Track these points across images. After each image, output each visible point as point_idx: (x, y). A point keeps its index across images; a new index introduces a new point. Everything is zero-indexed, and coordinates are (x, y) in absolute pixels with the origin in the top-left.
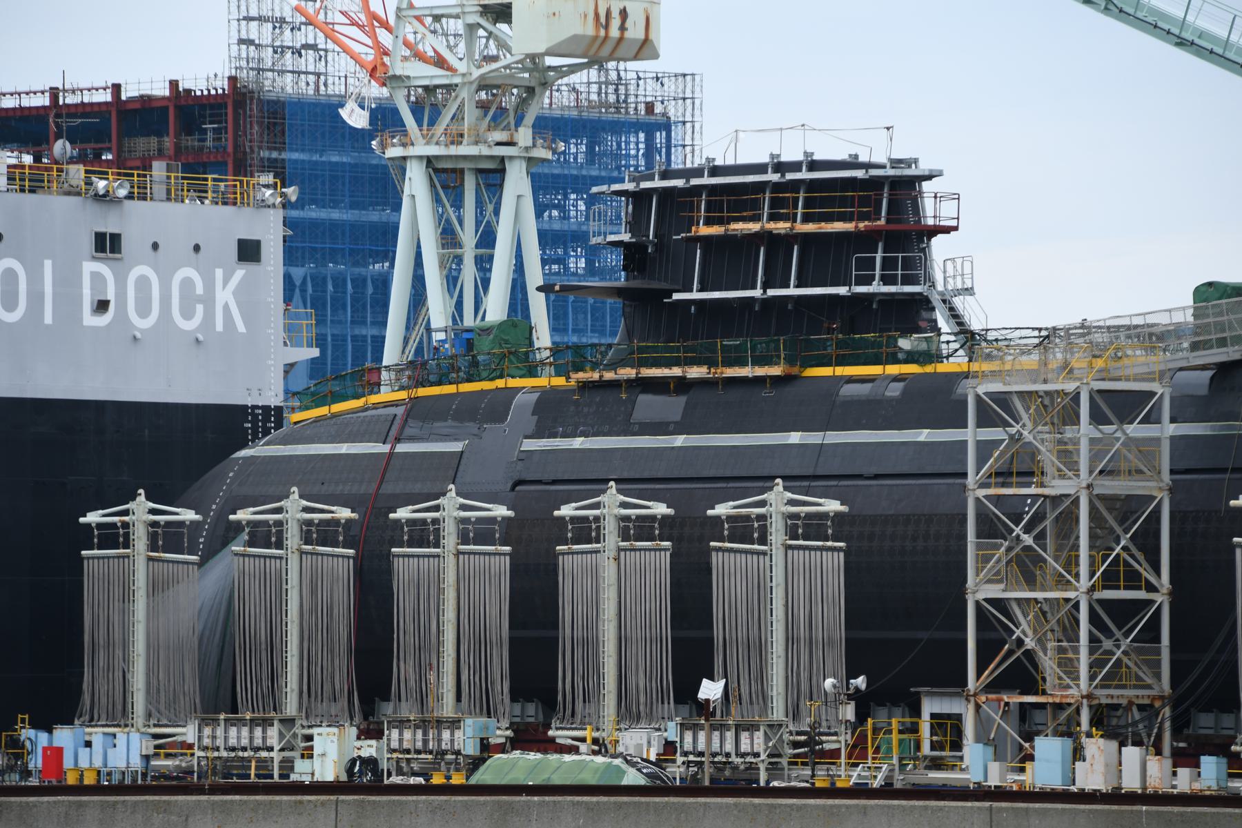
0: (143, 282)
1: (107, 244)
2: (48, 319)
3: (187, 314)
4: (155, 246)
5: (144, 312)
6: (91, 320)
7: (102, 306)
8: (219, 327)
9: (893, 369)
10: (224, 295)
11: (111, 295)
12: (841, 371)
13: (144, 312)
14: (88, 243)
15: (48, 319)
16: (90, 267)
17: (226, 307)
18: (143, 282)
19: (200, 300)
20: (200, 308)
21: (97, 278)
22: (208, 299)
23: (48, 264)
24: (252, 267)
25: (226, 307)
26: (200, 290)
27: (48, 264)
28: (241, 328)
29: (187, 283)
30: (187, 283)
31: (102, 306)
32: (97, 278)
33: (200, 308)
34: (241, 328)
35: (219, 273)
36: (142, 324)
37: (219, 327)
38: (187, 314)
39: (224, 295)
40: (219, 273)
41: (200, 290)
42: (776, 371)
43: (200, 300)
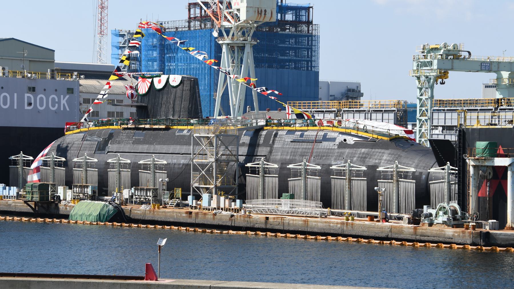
0: (41, 99)
1: (32, 90)
2: (15, 107)
3: (53, 106)
4: (45, 90)
5: (41, 105)
6: (27, 107)
7: (30, 104)
8: (62, 109)
10: (63, 102)
11: (33, 102)
13: (41, 105)
15: (15, 107)
16: (27, 95)
17: (64, 104)
18: (41, 99)
19: (57, 103)
20: (57, 105)
21: (29, 98)
22: (59, 103)
23: (16, 94)
24: (71, 95)
25: (64, 104)
26: (57, 100)
27: (16, 94)
28: (68, 109)
29: (53, 99)
30: (53, 99)
31: (30, 104)
32: (29, 98)
33: (57, 105)
34: (68, 109)
35: (62, 96)
37: (62, 109)
38: (53, 106)
39: (63, 102)
40: (62, 96)
41: (57, 100)
42: (164, 127)
43: (57, 103)
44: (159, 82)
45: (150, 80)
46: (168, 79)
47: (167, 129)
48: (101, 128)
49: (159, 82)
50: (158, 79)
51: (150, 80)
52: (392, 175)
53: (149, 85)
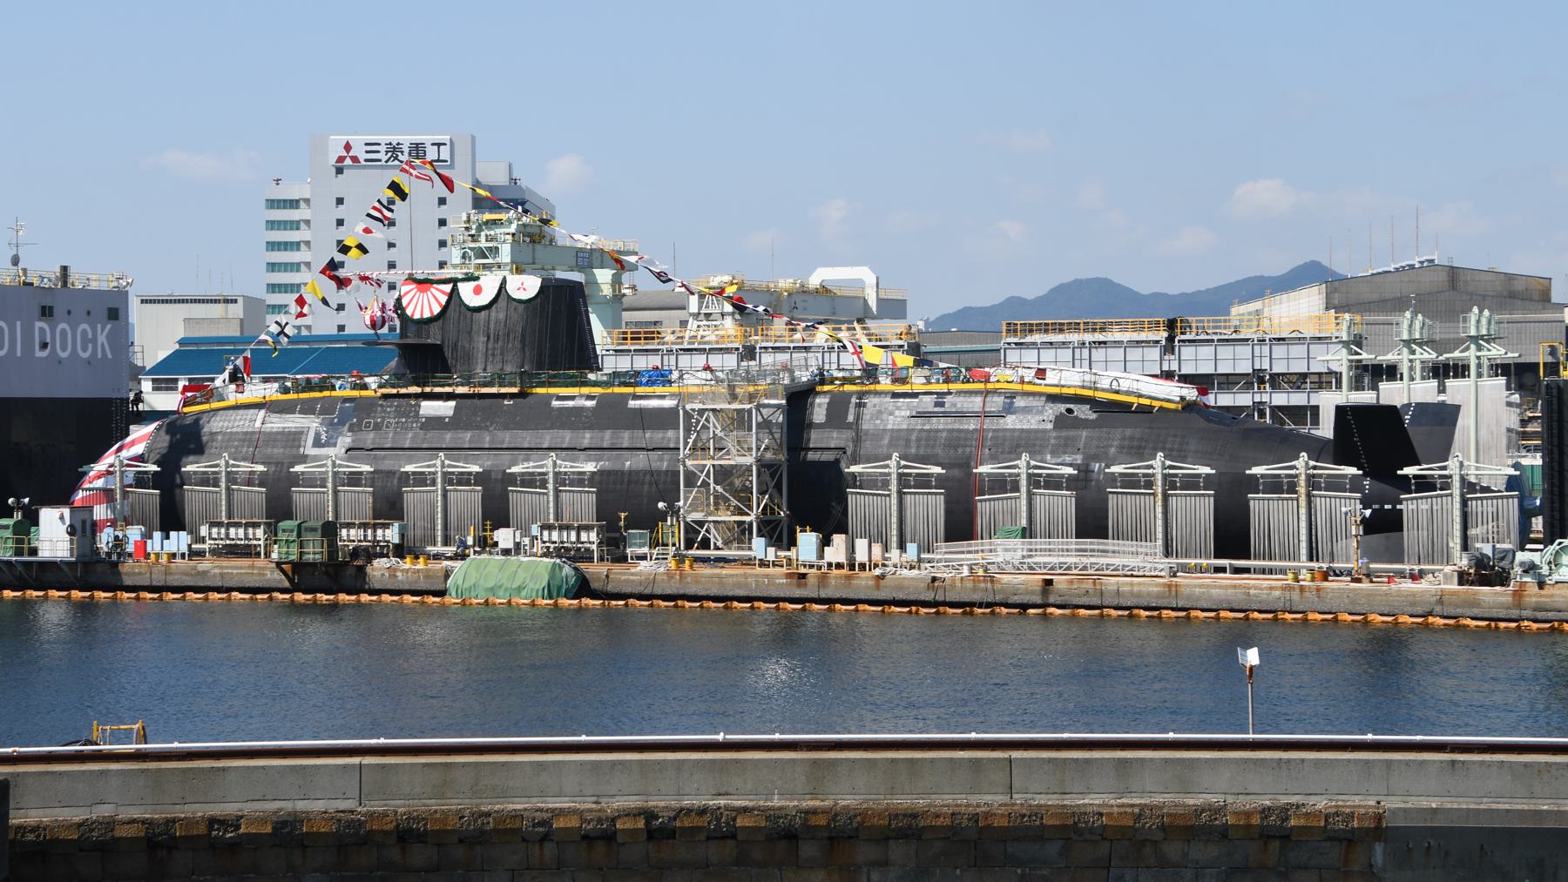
1: (47, 312)
3: (85, 350)
5: (64, 349)
6: (39, 354)
7: (44, 346)
9: (586, 390)
10: (102, 339)
12: (552, 390)
13: (64, 349)
14: (37, 311)
16: (39, 324)
18: (63, 332)
21: (42, 330)
22: (94, 341)
29: (84, 331)
30: (84, 331)
31: (44, 346)
32: (42, 330)
36: (64, 355)
38: (85, 350)
39: (102, 339)
42: (515, 390)
44: (478, 290)
45: (448, 288)
46: (504, 281)
47: (522, 395)
48: (302, 396)
49: (478, 290)
50: (472, 284)
51: (448, 288)
52: (1017, 482)
53: (444, 299)
